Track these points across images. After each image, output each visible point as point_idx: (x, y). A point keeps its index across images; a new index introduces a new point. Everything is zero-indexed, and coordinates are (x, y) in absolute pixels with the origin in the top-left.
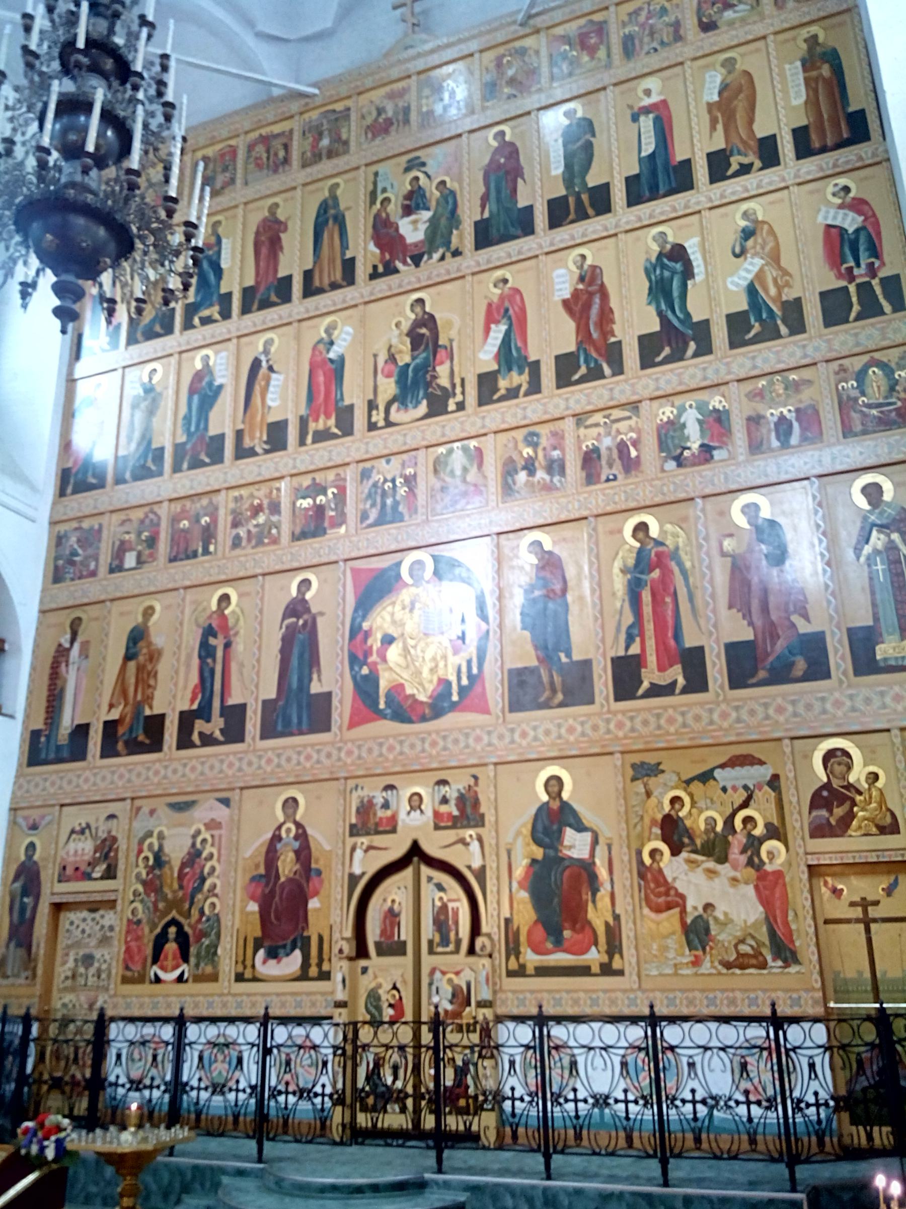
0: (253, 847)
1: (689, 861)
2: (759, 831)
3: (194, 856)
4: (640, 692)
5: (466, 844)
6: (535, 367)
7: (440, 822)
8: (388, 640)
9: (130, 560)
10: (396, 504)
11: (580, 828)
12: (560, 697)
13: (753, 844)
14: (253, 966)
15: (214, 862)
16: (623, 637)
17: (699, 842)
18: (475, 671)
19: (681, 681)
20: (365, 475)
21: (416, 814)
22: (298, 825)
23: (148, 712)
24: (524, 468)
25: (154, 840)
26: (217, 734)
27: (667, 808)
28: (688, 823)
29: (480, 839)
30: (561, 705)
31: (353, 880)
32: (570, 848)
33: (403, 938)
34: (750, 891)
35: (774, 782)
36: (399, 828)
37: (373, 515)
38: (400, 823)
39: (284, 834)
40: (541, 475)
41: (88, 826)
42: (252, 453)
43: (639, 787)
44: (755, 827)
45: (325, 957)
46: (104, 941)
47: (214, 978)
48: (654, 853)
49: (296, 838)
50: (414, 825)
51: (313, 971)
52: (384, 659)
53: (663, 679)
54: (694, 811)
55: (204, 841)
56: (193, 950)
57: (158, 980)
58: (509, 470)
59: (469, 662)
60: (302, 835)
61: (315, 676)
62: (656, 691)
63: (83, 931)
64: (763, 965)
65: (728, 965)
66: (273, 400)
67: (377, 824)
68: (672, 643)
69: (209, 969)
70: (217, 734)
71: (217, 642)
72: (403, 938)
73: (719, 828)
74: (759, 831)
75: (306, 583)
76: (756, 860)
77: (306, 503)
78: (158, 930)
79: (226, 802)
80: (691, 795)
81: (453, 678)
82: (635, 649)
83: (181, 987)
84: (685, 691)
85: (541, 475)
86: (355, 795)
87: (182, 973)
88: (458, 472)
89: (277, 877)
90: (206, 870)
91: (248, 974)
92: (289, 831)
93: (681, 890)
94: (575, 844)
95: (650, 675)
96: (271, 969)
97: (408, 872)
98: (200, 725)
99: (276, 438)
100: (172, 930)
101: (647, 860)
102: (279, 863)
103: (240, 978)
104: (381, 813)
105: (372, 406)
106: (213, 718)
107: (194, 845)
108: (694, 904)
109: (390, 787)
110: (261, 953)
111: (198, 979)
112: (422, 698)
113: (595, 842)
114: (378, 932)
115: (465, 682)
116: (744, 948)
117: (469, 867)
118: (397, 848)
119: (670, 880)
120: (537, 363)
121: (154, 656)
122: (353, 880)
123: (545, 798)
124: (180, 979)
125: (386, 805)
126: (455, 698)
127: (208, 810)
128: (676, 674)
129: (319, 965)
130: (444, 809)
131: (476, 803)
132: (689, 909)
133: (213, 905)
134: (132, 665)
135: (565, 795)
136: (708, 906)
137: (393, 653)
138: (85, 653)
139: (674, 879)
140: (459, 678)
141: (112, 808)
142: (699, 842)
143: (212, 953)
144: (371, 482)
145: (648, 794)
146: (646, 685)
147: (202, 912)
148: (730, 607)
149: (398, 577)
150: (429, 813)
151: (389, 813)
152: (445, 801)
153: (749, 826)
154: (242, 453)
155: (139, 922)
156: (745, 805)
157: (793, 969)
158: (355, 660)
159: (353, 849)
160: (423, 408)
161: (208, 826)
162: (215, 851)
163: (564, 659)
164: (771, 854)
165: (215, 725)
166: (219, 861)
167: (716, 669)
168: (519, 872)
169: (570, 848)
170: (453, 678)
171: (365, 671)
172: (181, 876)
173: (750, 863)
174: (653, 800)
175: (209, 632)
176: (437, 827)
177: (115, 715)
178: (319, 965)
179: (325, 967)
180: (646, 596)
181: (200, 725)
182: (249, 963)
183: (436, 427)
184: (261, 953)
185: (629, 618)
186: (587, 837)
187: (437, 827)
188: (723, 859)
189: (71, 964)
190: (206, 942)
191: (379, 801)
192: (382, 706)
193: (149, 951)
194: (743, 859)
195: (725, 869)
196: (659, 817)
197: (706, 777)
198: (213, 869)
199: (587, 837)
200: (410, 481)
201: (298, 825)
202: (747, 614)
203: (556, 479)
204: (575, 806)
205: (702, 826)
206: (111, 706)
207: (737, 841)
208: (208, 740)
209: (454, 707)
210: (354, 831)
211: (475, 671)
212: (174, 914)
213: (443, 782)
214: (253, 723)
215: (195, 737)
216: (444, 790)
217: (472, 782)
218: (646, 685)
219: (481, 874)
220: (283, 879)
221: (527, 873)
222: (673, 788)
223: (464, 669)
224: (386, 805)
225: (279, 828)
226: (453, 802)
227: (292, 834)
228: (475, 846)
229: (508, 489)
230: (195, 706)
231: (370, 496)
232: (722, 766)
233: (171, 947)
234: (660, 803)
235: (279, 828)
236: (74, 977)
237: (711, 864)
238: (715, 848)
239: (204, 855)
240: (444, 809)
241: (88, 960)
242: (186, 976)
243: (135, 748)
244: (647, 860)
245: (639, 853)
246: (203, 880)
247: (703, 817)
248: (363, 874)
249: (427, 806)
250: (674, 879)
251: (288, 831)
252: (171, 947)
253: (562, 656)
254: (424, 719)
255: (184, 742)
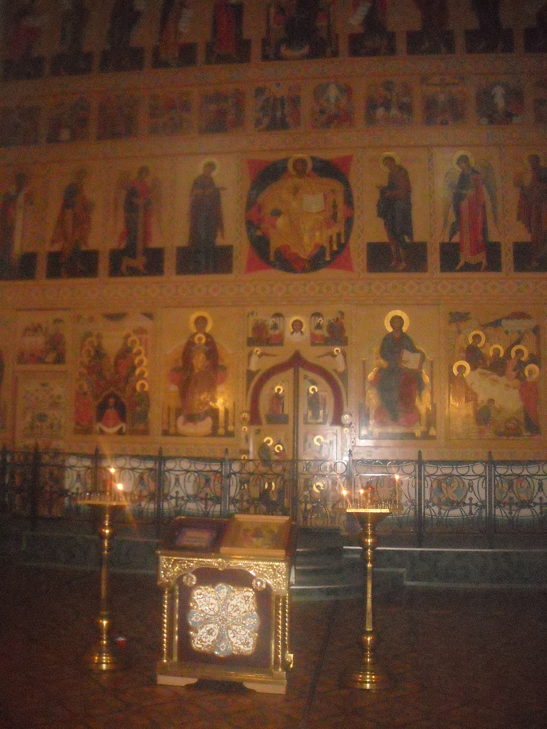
0: (172, 348)
1: (481, 374)
2: (525, 358)
3: (126, 352)
4: (458, 267)
5: (335, 356)
6: (392, 37)
7: (315, 341)
8: (277, 213)
9: (65, 134)
10: (284, 116)
11: (413, 350)
12: (404, 265)
13: (521, 365)
14: (176, 426)
15: (142, 356)
16: (448, 230)
17: (488, 363)
18: (343, 241)
19: (484, 262)
20: (260, 91)
21: (297, 335)
22: (208, 336)
23: (84, 248)
24: (382, 105)
25: (94, 339)
26: (141, 267)
27: (471, 341)
28: (483, 351)
29: (344, 354)
30: (404, 270)
31: (250, 375)
32: (406, 362)
33: (286, 412)
34: (516, 393)
35: (536, 330)
36: (285, 343)
37: (266, 121)
38: (286, 340)
39: (196, 341)
40: (394, 112)
41: (40, 326)
42: (165, 65)
43: (454, 328)
44: (523, 356)
45: (230, 423)
46: (55, 405)
47: (145, 432)
48: (461, 369)
49: (206, 344)
50: (296, 340)
51: (221, 431)
52: (274, 227)
53: (473, 260)
54: (488, 344)
55: (134, 342)
56: (128, 415)
57: (102, 432)
58: (371, 105)
59: (339, 235)
60: (211, 343)
61: (219, 234)
62: (468, 268)
63: (37, 398)
64: (519, 435)
65: (501, 434)
66: (184, 26)
67: (268, 340)
68: (480, 238)
69: (141, 427)
70: (141, 267)
71: (140, 201)
72: (286, 412)
73: (501, 355)
74: (525, 358)
75: (211, 166)
76: (522, 375)
77: (213, 107)
78: (100, 400)
79: (149, 316)
80: (486, 334)
81: (326, 245)
82: (456, 239)
83: (120, 438)
84: (487, 269)
85: (394, 112)
86: (251, 318)
87: (121, 429)
88: (333, 100)
89: (192, 370)
90: (136, 362)
91: (172, 430)
92: (201, 339)
93: (476, 391)
94: (410, 360)
95: (465, 257)
96: (190, 429)
97: (290, 372)
98: (127, 262)
99: (187, 56)
100: (112, 401)
101: (455, 371)
102: (194, 361)
103: (166, 433)
104: (271, 332)
105: (265, 42)
106: (138, 258)
107: (125, 344)
108: (482, 398)
109: (278, 315)
110: (181, 419)
111: (133, 432)
112: (302, 256)
113: (423, 359)
114: (267, 408)
115: (335, 247)
116: (510, 425)
117: (335, 371)
118: (282, 354)
119: (469, 384)
120: (393, 34)
121: (88, 208)
122: (250, 375)
123: (390, 330)
124: (120, 432)
125: (275, 327)
126: (328, 259)
127: (135, 321)
128: (481, 258)
129: (226, 427)
130: (318, 332)
131: (342, 330)
132: (479, 402)
133: (143, 385)
134: (69, 212)
135: (404, 329)
136: (491, 401)
137: (281, 222)
138: (29, 199)
139: (472, 384)
140: (331, 246)
141: (59, 315)
142: (488, 363)
143: (144, 416)
144: (264, 97)
145: (459, 332)
146: (461, 263)
147: (134, 389)
148: (519, 219)
149: (285, 169)
150: (307, 334)
151: (277, 332)
152: (319, 326)
153: (520, 355)
154: (159, 63)
155: (85, 394)
156: (518, 342)
157: (537, 437)
158: (251, 225)
159: (250, 355)
160: (306, 50)
161: (135, 332)
162: (141, 348)
163: (407, 240)
164: (531, 372)
165: (140, 261)
166: (146, 355)
167: (507, 258)
168: (371, 376)
169: (406, 362)
170: (326, 245)
171: (259, 233)
172: (116, 364)
173: (518, 377)
174: (462, 337)
175: (132, 193)
176: (313, 344)
177: (57, 248)
178: (226, 427)
179: (230, 428)
180: (465, 204)
181: (127, 262)
182: (172, 424)
183: (316, 67)
184: (181, 419)
185: (452, 218)
186: (418, 356)
187: (313, 344)
188: (502, 373)
189: (28, 419)
190: (138, 409)
191: (270, 322)
192: (272, 259)
193: (93, 413)
194: (514, 374)
195: (503, 380)
196: (465, 346)
197: (496, 324)
198: (141, 362)
199: (418, 356)
200: (295, 101)
201: (208, 336)
202: (529, 226)
203: (405, 116)
204: (411, 336)
205: (491, 353)
206: (53, 242)
207: (511, 364)
208: (133, 272)
209: (327, 264)
210: (251, 342)
211: (343, 241)
212: (112, 389)
213: (318, 315)
214: (170, 262)
215: (123, 268)
216: (319, 320)
217: (339, 316)
218: (461, 263)
219: (344, 375)
220: (197, 371)
221: (375, 376)
222: (475, 329)
223: (335, 238)
224: (275, 327)
225: (193, 335)
226: (325, 328)
227: (204, 341)
228: (340, 358)
229: (370, 119)
230: (123, 246)
231: (263, 108)
232: (508, 318)
233: (111, 412)
234: (466, 339)
235: (193, 335)
236: (32, 428)
237: (495, 376)
238: (498, 366)
239: (135, 350)
240: (318, 332)
241: (42, 417)
242: (124, 430)
243: (74, 273)
244: (455, 371)
245: (451, 367)
246: (134, 368)
247: (493, 348)
248: (258, 371)
249: (305, 328)
250: (472, 384)
251: (200, 339)
252: (111, 412)
253: (406, 237)
254: (304, 270)
255: (115, 270)
